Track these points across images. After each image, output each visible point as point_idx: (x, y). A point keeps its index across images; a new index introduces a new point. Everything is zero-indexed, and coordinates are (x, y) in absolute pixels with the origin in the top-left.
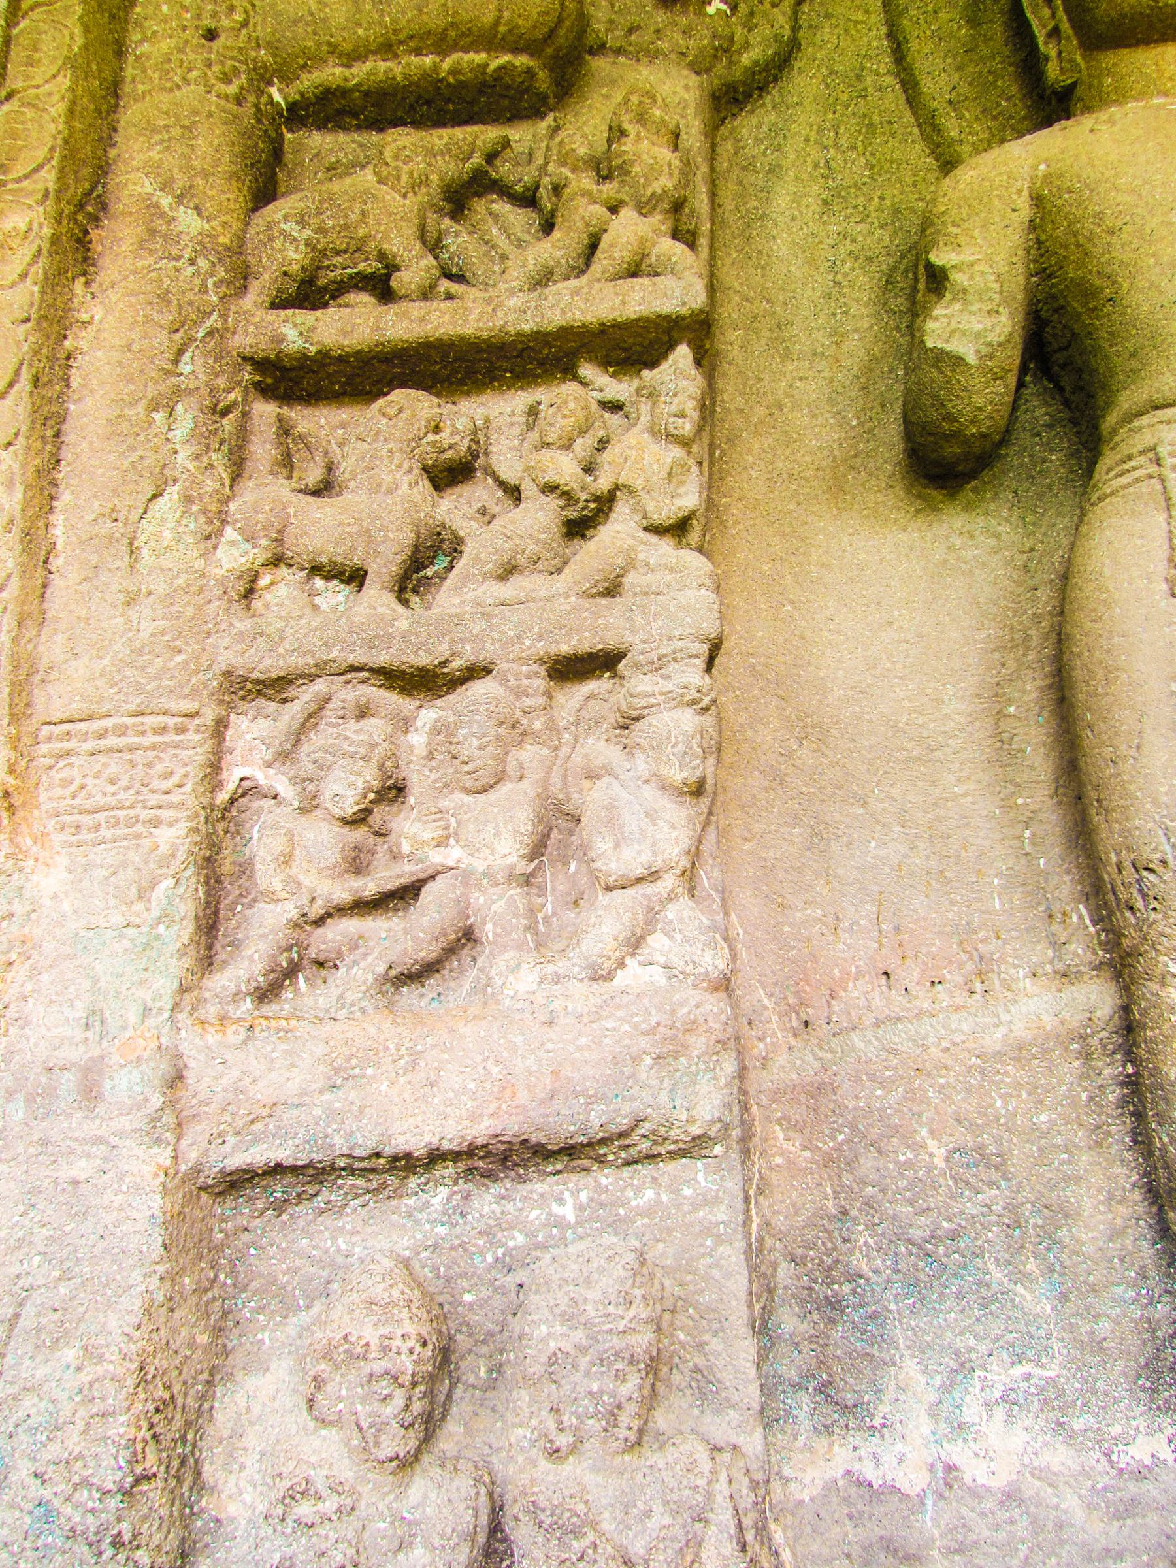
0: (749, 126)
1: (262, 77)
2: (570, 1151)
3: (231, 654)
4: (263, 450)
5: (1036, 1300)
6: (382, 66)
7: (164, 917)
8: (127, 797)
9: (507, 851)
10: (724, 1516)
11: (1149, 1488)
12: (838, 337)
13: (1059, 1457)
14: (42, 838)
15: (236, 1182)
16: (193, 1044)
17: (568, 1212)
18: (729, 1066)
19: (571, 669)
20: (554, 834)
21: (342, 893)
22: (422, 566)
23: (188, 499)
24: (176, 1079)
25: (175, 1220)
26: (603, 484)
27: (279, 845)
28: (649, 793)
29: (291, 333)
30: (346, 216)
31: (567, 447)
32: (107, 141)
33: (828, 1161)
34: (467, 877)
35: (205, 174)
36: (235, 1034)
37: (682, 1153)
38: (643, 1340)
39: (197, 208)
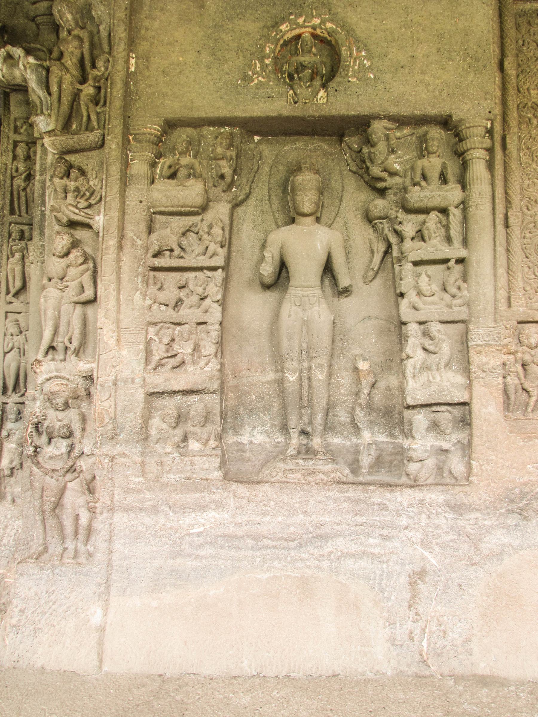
1: (149, 208)
2: (197, 392)
3: (148, 319)
4: (151, 281)
5: (267, 418)
7: (141, 358)
9: (189, 350)
12: (252, 255)
13: (267, 440)
14: (123, 346)
15: (152, 394)
16: (146, 376)
18: (219, 382)
19: (199, 324)
20: (196, 348)
24: (144, 380)
25: (145, 398)
26: (206, 294)
27: (156, 348)
28: (210, 343)
29: (156, 263)
31: (201, 286)
32: (124, 223)
33: (237, 397)
34: (184, 354)
35: (141, 232)
36: (152, 375)
37: (211, 393)
38: (205, 414)
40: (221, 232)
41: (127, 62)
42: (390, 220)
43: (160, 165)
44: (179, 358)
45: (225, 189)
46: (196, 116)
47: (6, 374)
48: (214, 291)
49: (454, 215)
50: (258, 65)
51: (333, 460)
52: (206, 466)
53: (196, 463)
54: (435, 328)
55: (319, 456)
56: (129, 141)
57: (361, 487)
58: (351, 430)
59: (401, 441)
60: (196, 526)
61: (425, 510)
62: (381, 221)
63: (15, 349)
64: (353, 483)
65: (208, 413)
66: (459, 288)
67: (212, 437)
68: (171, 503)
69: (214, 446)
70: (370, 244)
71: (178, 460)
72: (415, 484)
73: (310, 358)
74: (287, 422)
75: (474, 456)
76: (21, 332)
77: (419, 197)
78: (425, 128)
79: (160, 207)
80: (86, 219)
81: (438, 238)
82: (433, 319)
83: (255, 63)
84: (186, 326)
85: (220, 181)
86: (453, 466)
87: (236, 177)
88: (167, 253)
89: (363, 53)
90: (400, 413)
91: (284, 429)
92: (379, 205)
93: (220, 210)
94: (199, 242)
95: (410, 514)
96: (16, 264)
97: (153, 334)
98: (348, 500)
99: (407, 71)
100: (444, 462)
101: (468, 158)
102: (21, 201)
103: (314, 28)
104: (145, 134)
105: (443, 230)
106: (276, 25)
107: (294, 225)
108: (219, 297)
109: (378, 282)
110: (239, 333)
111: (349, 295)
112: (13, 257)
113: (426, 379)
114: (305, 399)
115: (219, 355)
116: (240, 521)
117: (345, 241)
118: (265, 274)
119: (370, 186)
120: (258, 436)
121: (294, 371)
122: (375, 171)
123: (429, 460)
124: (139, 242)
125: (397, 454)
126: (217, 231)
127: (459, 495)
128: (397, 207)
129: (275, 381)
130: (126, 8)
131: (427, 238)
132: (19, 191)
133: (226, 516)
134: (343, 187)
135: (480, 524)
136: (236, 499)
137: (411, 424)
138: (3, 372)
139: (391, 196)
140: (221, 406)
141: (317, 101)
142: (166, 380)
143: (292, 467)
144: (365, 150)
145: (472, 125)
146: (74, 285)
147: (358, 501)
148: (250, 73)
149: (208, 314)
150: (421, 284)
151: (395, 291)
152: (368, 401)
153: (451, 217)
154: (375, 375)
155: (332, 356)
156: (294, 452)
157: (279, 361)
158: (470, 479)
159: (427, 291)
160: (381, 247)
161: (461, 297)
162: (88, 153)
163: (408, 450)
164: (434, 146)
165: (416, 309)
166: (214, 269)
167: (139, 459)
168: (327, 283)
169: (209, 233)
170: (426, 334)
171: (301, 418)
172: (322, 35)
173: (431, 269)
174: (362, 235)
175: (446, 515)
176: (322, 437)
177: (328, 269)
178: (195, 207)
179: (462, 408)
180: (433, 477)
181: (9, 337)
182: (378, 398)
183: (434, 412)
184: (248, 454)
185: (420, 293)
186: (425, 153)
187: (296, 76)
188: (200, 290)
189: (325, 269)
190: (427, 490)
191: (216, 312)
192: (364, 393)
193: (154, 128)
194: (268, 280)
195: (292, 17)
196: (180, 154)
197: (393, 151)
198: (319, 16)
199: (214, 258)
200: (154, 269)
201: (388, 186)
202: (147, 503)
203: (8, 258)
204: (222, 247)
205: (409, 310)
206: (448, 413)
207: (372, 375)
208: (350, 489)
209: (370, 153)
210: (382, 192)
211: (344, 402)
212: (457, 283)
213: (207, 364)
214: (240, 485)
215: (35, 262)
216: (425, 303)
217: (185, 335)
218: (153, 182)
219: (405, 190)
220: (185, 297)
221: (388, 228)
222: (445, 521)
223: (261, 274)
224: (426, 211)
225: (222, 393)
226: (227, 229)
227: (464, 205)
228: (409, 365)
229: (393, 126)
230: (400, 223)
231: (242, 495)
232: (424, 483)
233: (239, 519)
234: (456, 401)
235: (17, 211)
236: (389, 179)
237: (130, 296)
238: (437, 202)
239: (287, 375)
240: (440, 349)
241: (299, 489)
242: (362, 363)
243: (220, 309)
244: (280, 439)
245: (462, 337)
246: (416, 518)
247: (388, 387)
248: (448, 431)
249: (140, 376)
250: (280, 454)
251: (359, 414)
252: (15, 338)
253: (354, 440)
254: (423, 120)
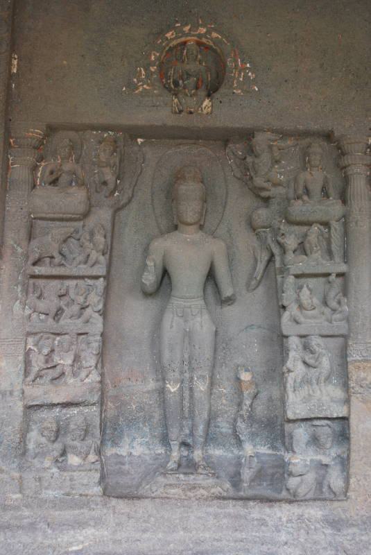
0: (123, 213)
3: (27, 330)
4: (31, 290)
5: (147, 429)
9: (69, 362)
10: (93, 448)
11: (160, 457)
13: (147, 452)
16: (24, 387)
17: (76, 412)
18: (100, 393)
20: (77, 359)
21: (45, 367)
22: (58, 313)
23: (20, 302)
24: (23, 393)
26: (87, 304)
28: (91, 355)
29: (36, 271)
31: (82, 295)
33: (117, 407)
38: (85, 428)
40: (103, 239)
41: (10, 64)
42: (274, 229)
43: (40, 169)
44: (58, 370)
45: (107, 194)
46: (79, 122)
48: (95, 299)
49: (336, 230)
50: (143, 72)
51: (214, 474)
52: (85, 482)
53: (75, 478)
54: (315, 342)
55: (200, 471)
56: (10, 143)
57: (240, 503)
58: (233, 441)
59: (283, 453)
60: (75, 544)
61: (304, 525)
62: (264, 230)
64: (234, 499)
65: (88, 426)
66: (339, 303)
67: (92, 451)
68: (49, 520)
69: (93, 460)
70: (254, 252)
71: (56, 475)
72: (293, 499)
73: (192, 370)
74: (167, 433)
75: (352, 470)
77: (301, 211)
78: (308, 140)
81: (319, 252)
82: (312, 333)
83: (141, 70)
84: (67, 336)
85: (103, 187)
86: (332, 481)
87: (118, 181)
88: (48, 259)
89: (248, 65)
90: (282, 425)
91: (165, 440)
92: (262, 215)
93: (103, 215)
94: (80, 249)
95: (290, 530)
97: (32, 344)
98: (228, 515)
99: (290, 85)
100: (324, 477)
101: (350, 173)
103: (200, 36)
104: (27, 138)
105: (325, 243)
106: (161, 33)
107: (177, 232)
108: (100, 307)
109: (261, 290)
110: (120, 341)
111: (232, 304)
113: (307, 393)
114: (186, 411)
115: (99, 366)
116: (120, 538)
117: (228, 248)
118: (147, 283)
119: (254, 193)
120: (138, 447)
121: (176, 382)
122: (259, 182)
123: (309, 474)
124: (20, 250)
125: (277, 467)
126: (99, 238)
127: (337, 509)
128: (280, 217)
129: (156, 390)
130: (9, 8)
131: (308, 252)
133: (106, 532)
134: (227, 193)
135: (357, 539)
136: (116, 515)
137: (292, 438)
139: (274, 207)
140: (101, 419)
141: (202, 110)
142: (45, 393)
143: (173, 482)
144: (249, 159)
145: (353, 141)
147: (237, 517)
148: (135, 80)
149: (89, 324)
150: (302, 297)
151: (278, 300)
152: (250, 412)
153: (333, 230)
154: (257, 385)
155: (214, 366)
156: (175, 466)
157: (161, 373)
158: (348, 494)
159: (309, 304)
160: (265, 257)
161: (341, 312)
163: (289, 464)
164: (316, 159)
165: (297, 323)
166: (97, 278)
167: (16, 475)
168: (210, 290)
169: (91, 240)
170: (306, 347)
171: (181, 430)
172: (208, 43)
173: (312, 282)
174: (245, 242)
175: (324, 530)
176: (203, 449)
177: (211, 276)
178: (77, 214)
179: (342, 422)
180: (312, 492)
182: (260, 410)
183: (314, 426)
184: (127, 467)
185: (301, 307)
186: (308, 165)
187: (181, 82)
188: (81, 299)
189: (207, 277)
190: (306, 505)
191: (97, 325)
192: (246, 405)
193: (37, 132)
194: (150, 289)
195: (177, 25)
196: (62, 159)
197: (277, 162)
198: (204, 25)
199: (96, 267)
200: (34, 277)
201: (271, 196)
202: (25, 521)
204: (103, 255)
205: (289, 323)
206: (327, 428)
207: (254, 387)
208: (231, 505)
209: (253, 162)
210: (266, 200)
211: (226, 413)
212: (338, 297)
213: (87, 376)
214: (120, 501)
216: (306, 317)
217: (65, 345)
218: (34, 186)
219: (288, 200)
220: (65, 305)
221: (272, 238)
222: (323, 537)
223: (143, 283)
224: (309, 224)
225: (102, 405)
226: (109, 235)
227: (345, 219)
228: (290, 379)
229: (277, 138)
230: (283, 234)
231: (122, 511)
232: (303, 498)
233: (118, 536)
234: (335, 415)
236: (273, 189)
237: (9, 305)
238: (318, 217)
239: (168, 386)
240: (320, 363)
241: (179, 504)
242: (244, 374)
243: (100, 319)
244: (160, 450)
245: (342, 351)
246: (295, 534)
247: (271, 397)
248: (328, 446)
249: (19, 388)
250: (160, 468)
251: (241, 425)
253: (236, 452)
254: (307, 134)
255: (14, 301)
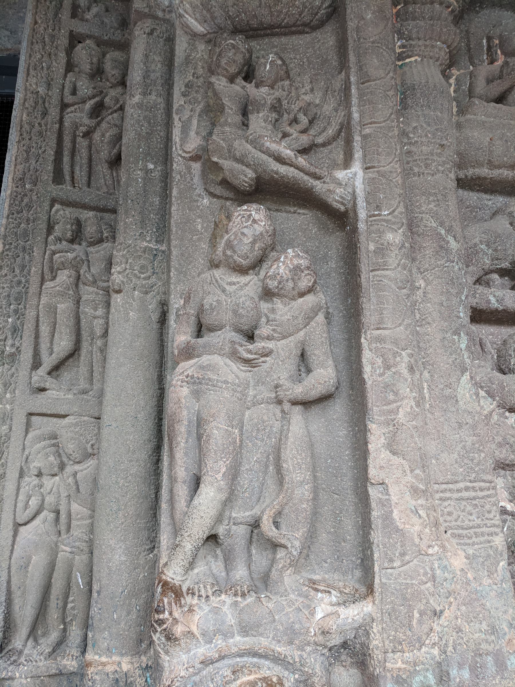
6: (506, 172)
8: (479, 521)
29: (493, 300)
30: (506, 245)
39: (454, 237)
47: (14, 587)
63: (45, 513)
76: (62, 467)
79: (481, 165)
80: (306, 178)
96: (62, 294)
102: (77, 158)
112: (54, 278)
124: (453, 244)
132: (75, 137)
138: (9, 582)
146: (285, 348)
162: (283, 39)
181: (31, 481)
203: (43, 281)
215: (127, 288)
235: (68, 178)
252: (48, 483)
255: (459, 373)
